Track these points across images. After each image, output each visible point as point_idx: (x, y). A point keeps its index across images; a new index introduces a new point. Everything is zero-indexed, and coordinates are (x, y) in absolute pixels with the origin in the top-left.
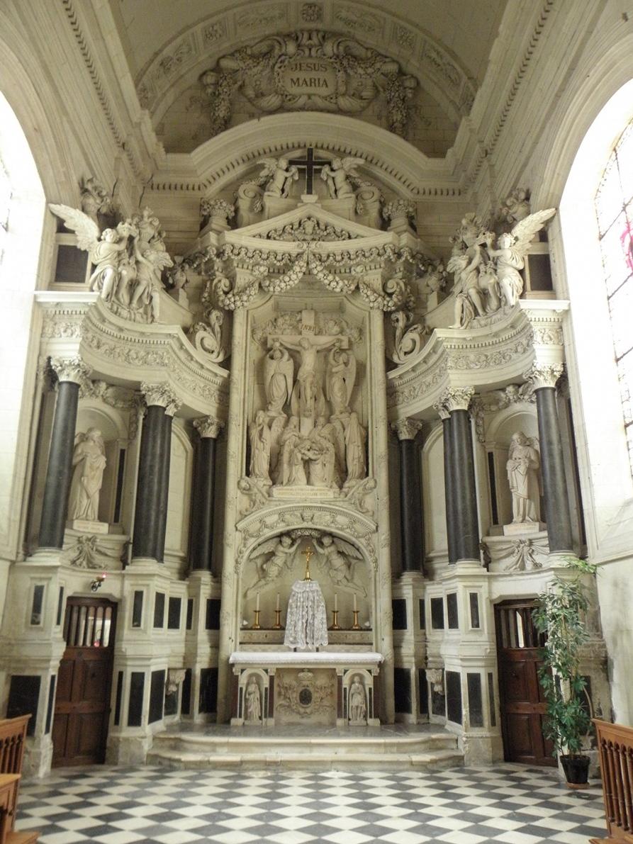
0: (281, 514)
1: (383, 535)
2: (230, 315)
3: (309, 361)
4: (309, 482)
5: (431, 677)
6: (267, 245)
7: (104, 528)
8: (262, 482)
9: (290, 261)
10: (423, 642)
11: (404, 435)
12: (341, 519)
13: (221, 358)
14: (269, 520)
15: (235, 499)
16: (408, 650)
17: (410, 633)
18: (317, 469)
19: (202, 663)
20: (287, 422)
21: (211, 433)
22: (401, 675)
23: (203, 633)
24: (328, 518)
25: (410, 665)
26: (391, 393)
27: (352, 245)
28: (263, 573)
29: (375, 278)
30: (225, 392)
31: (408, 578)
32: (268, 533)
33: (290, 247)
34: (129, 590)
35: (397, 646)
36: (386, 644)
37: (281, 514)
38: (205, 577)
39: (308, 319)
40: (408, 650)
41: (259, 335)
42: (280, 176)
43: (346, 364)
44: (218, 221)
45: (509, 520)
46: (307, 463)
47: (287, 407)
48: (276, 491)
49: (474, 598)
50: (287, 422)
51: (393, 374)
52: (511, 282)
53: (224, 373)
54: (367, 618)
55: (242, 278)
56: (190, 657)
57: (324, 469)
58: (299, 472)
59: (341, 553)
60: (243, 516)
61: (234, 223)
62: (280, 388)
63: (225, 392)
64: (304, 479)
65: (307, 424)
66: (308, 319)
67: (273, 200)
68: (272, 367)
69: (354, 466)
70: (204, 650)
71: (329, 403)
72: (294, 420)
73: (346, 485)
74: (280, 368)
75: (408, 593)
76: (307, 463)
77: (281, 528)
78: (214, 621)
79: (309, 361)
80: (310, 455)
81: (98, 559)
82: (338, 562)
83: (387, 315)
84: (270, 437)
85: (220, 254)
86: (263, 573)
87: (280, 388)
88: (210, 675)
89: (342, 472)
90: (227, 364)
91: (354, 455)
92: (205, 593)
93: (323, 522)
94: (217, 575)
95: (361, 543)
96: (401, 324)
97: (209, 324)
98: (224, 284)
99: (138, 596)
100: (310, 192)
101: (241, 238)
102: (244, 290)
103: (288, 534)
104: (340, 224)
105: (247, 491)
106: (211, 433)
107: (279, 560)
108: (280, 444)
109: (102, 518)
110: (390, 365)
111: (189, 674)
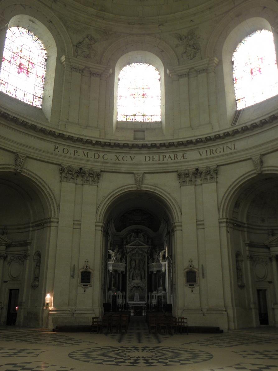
0: (134, 284)
1: (146, 287)
2: (126, 257)
3: (137, 261)
4: (137, 280)
5: (151, 305)
6: (132, 247)
7: (114, 287)
8: (131, 280)
9: (135, 248)
10: (151, 301)
11: (150, 274)
12: (141, 285)
13: (125, 263)
14: (132, 285)
15: (128, 282)
16: (149, 302)
17: (149, 300)
18: (138, 278)
19: (124, 303)
20: (134, 271)
21: (124, 273)
22: (148, 304)
23: (124, 300)
24: (139, 284)
25: (149, 303)
26: (148, 267)
27: (143, 247)
28: (131, 292)
29: (146, 250)
30: (126, 267)
31: (149, 293)
32: (132, 286)
33: (135, 247)
34: (117, 294)
35: (148, 301)
36: (147, 301)
37: (134, 284)
38: (124, 293)
39: (137, 255)
40: (149, 302)
41: (130, 257)
42: (133, 235)
43: (142, 262)
44: (125, 243)
45: (160, 287)
46: (137, 277)
47: (134, 268)
48: (133, 281)
49: (155, 296)
50: (134, 271)
51: (148, 265)
52: (161, 259)
53: (126, 265)
54: (145, 298)
55: (128, 250)
56: (123, 302)
57: (139, 278)
58: (136, 278)
59: (141, 289)
60: (129, 284)
61: (127, 243)
62: (133, 265)
63: (126, 267)
64: (136, 279)
65: (137, 270)
66: (137, 255)
67: (132, 239)
68: (132, 263)
69: (143, 277)
70: (124, 301)
71: (140, 268)
72: (135, 271)
73: (142, 280)
74: (133, 263)
75: (149, 294)
76: (137, 277)
77: (134, 286)
78: (125, 298)
79: (137, 261)
80: (137, 276)
81: (114, 291)
82: (141, 290)
83: (148, 257)
84: (132, 273)
85: (125, 248)
86: (131, 292)
87: (133, 265)
88: (125, 304)
89: (141, 278)
90: (126, 263)
91: (143, 275)
92: (124, 294)
93: (139, 285)
94: (126, 292)
95: (144, 288)
96: (150, 257)
97: (124, 258)
98: (126, 252)
99: (118, 295)
100: (137, 238)
101: (128, 246)
102: (129, 252)
103: (134, 287)
104: (141, 243)
105: (129, 281)
106: (124, 273)
107: (133, 290)
108: (133, 274)
109: (113, 286)
110: (148, 264)
111: (123, 304)
